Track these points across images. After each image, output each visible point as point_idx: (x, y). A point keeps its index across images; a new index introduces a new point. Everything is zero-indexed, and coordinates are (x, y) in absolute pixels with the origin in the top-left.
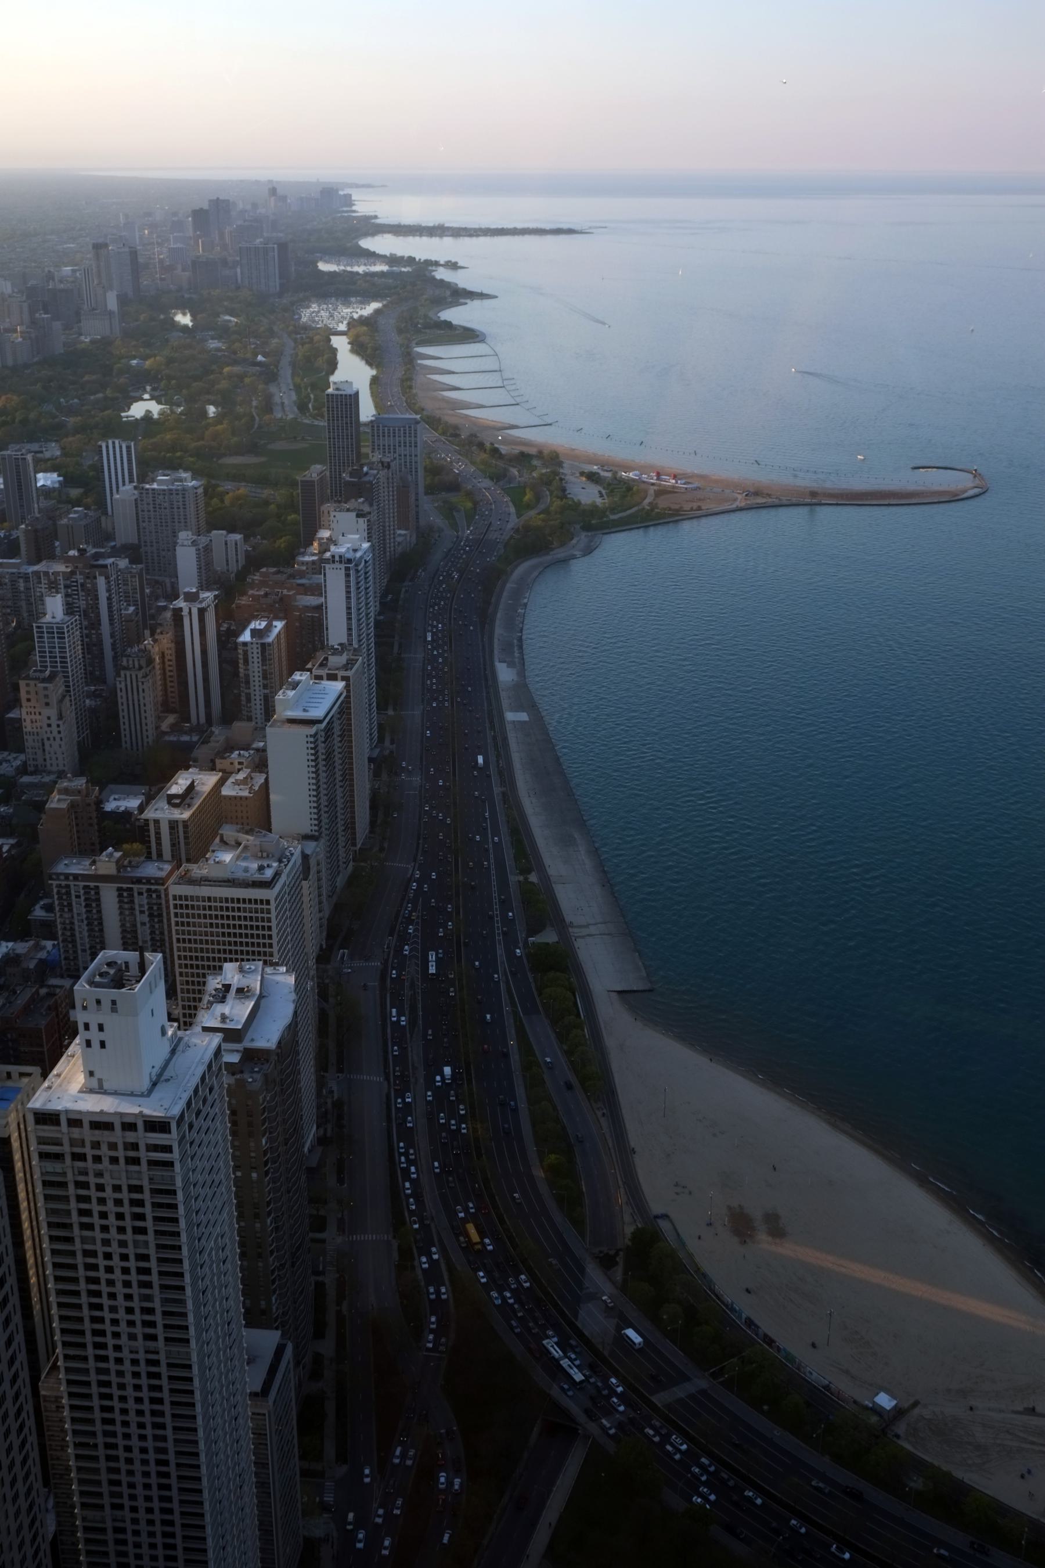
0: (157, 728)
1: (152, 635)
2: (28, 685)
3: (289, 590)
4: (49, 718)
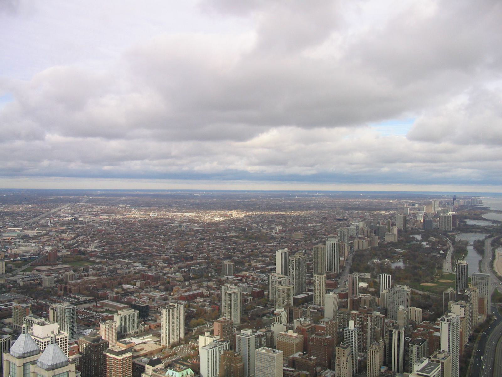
0: (379, 370)
1: (383, 338)
2: (339, 349)
3: (432, 329)
4: (344, 361)
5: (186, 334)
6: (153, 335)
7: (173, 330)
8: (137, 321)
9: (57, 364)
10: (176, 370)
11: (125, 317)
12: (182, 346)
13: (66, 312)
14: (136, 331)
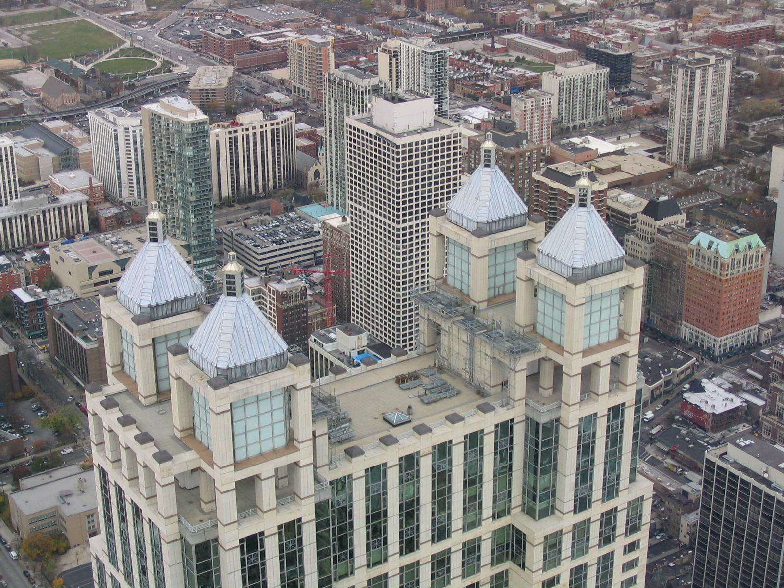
5: (729, 138)
6: (644, 134)
7: (701, 124)
8: (602, 93)
9: (595, 266)
10: (719, 236)
11: (572, 84)
12: (720, 168)
13: (423, 62)
14: (600, 118)
